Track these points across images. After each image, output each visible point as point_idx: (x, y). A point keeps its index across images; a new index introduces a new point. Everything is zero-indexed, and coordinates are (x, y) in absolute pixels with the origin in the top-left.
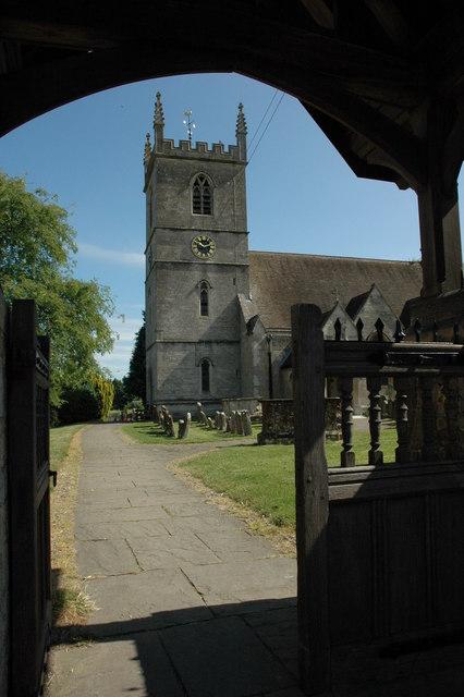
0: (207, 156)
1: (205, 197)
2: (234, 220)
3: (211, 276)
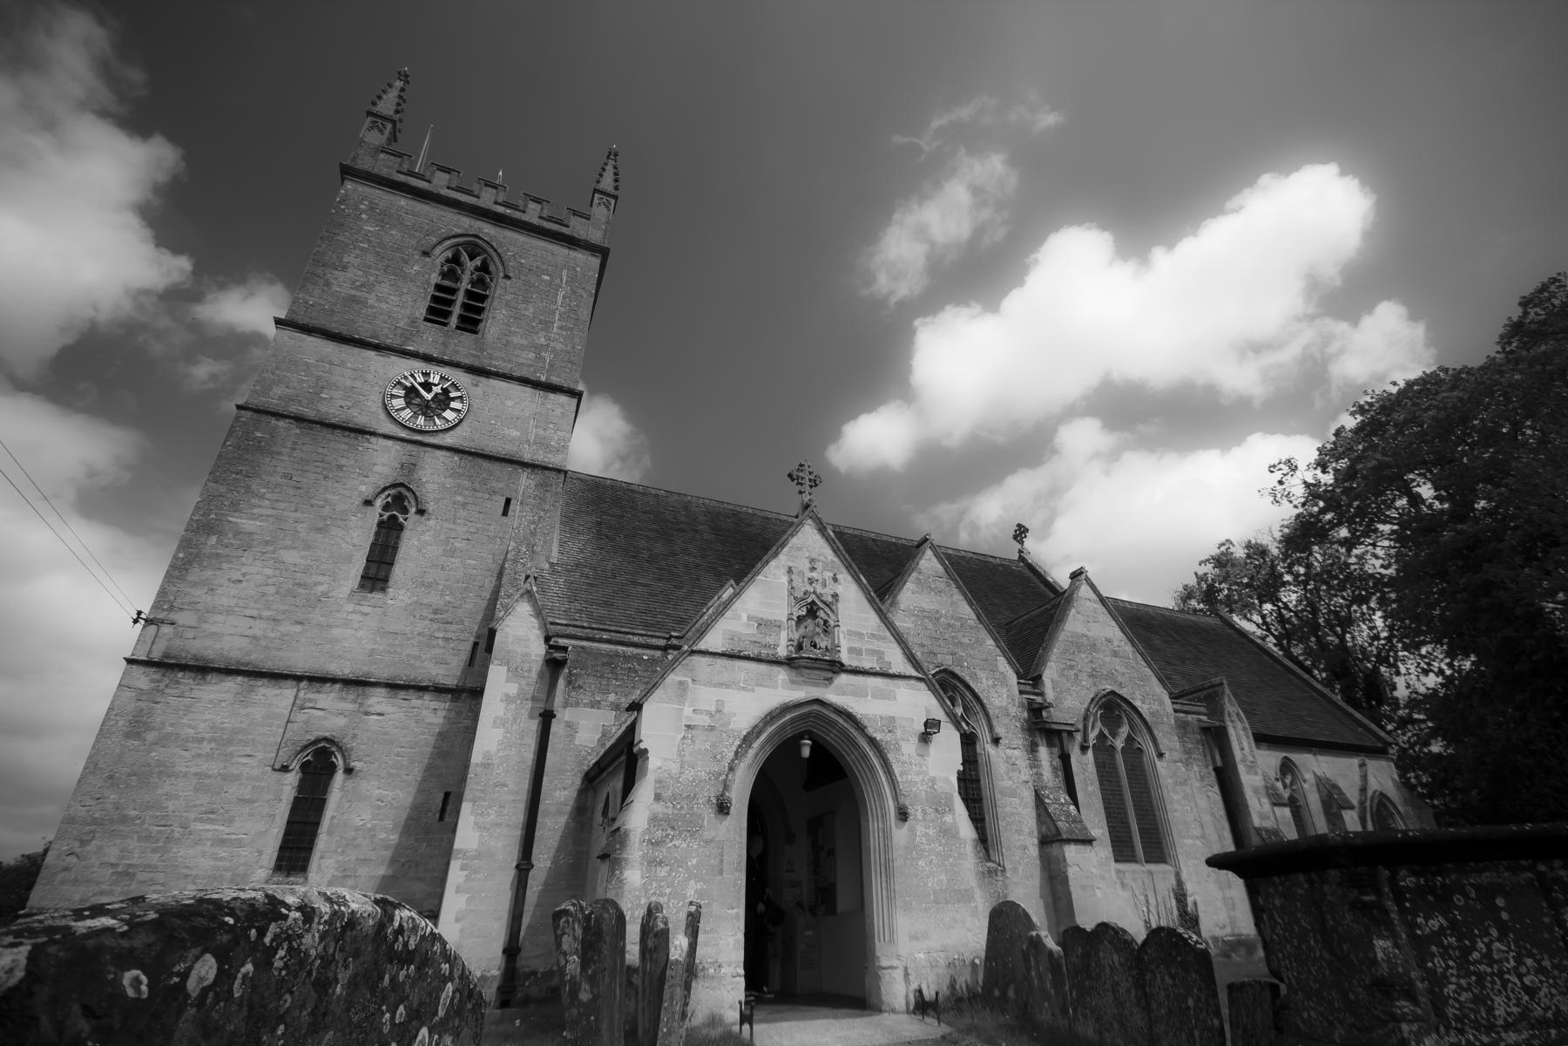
2: (539, 358)
3: (434, 474)
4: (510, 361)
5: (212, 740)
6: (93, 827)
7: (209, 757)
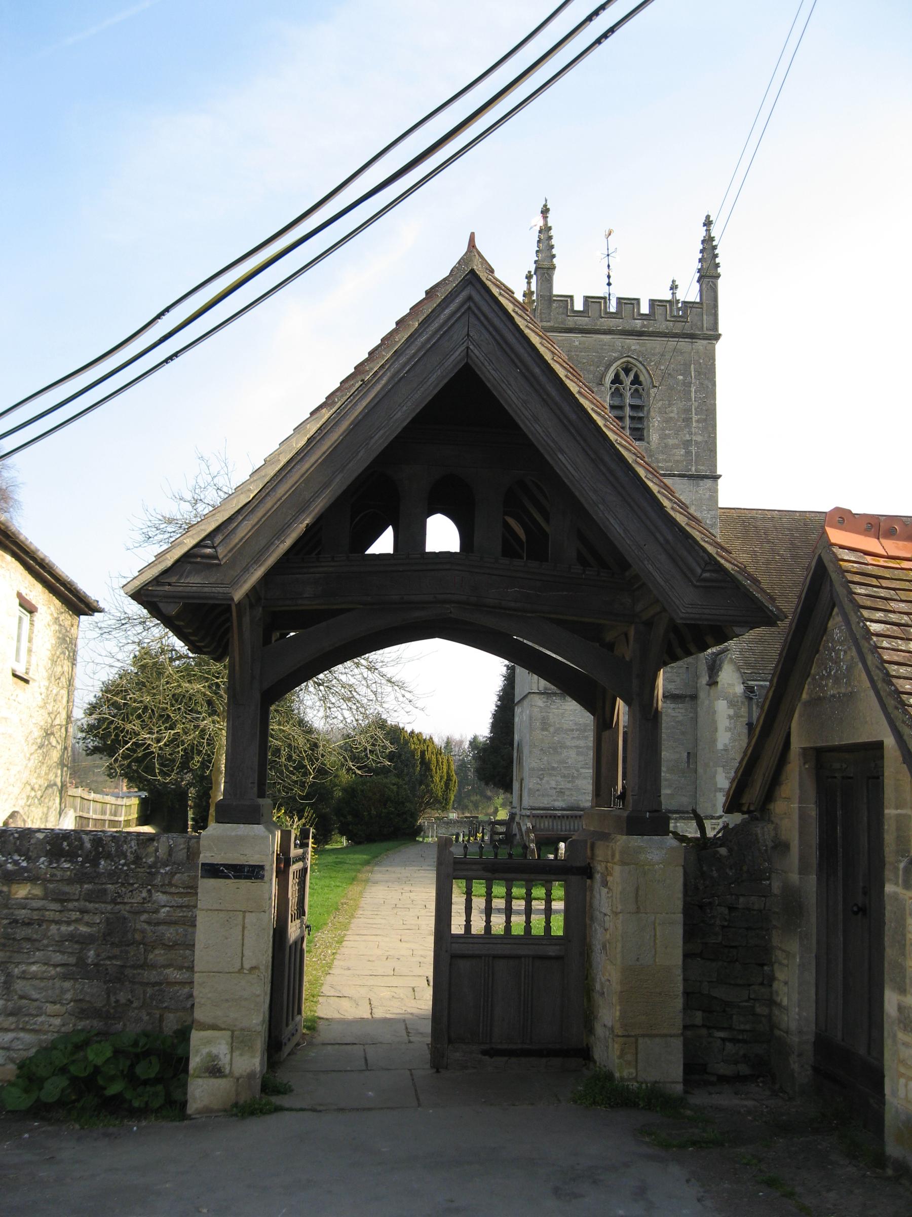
0: (638, 323)
1: (633, 407)
2: (688, 453)
4: (670, 461)
5: (577, 730)
6: (542, 772)
7: (578, 738)
